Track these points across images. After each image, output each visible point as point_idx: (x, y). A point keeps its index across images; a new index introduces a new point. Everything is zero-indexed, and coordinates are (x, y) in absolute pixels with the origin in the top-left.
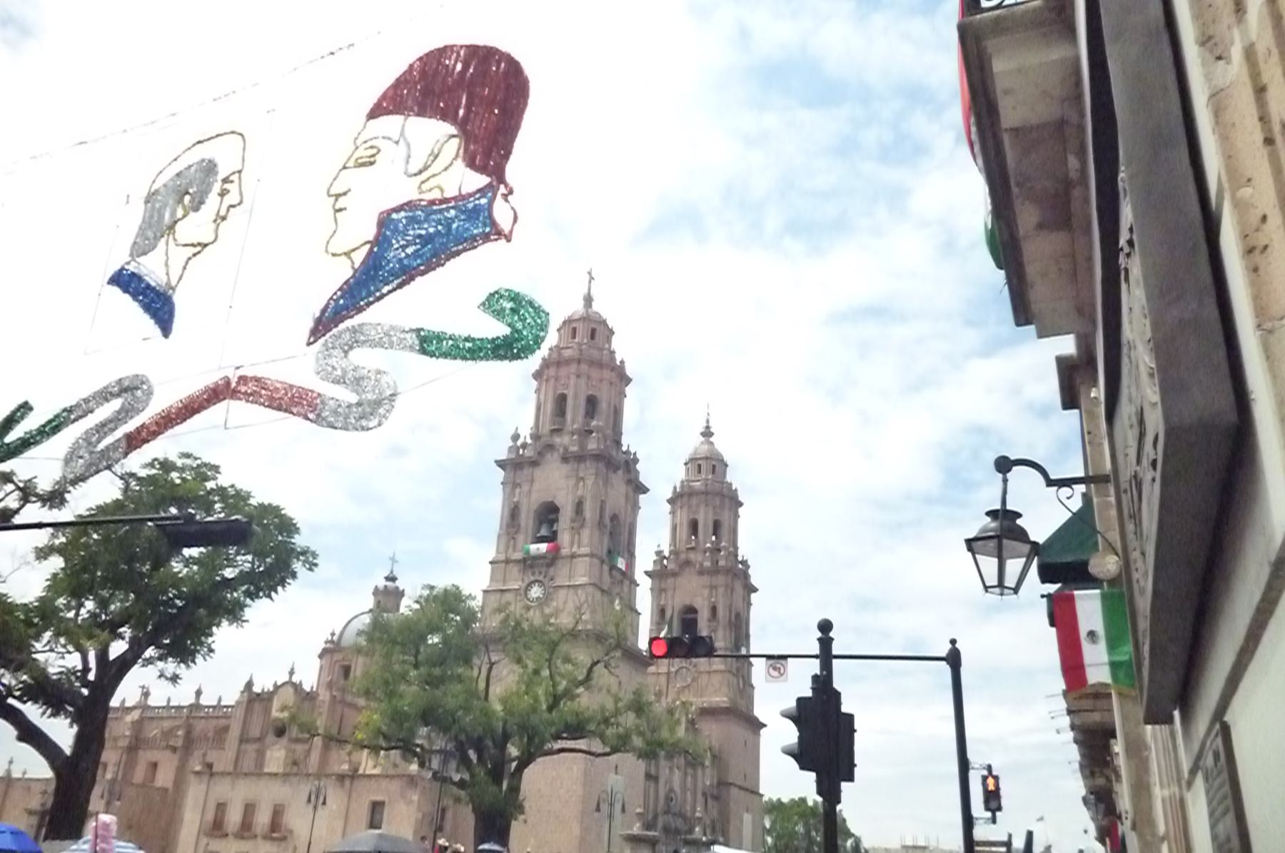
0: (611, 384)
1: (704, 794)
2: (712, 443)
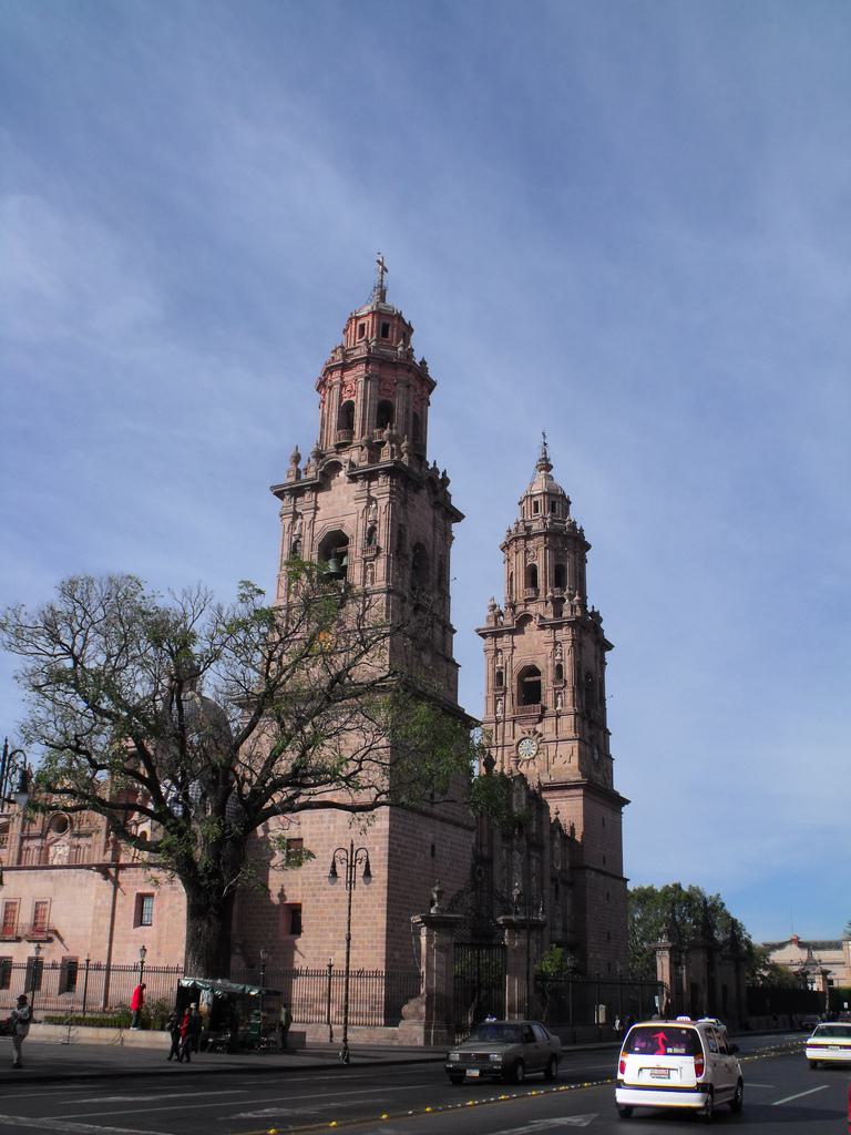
0: (408, 386)
1: (553, 880)
2: (551, 478)
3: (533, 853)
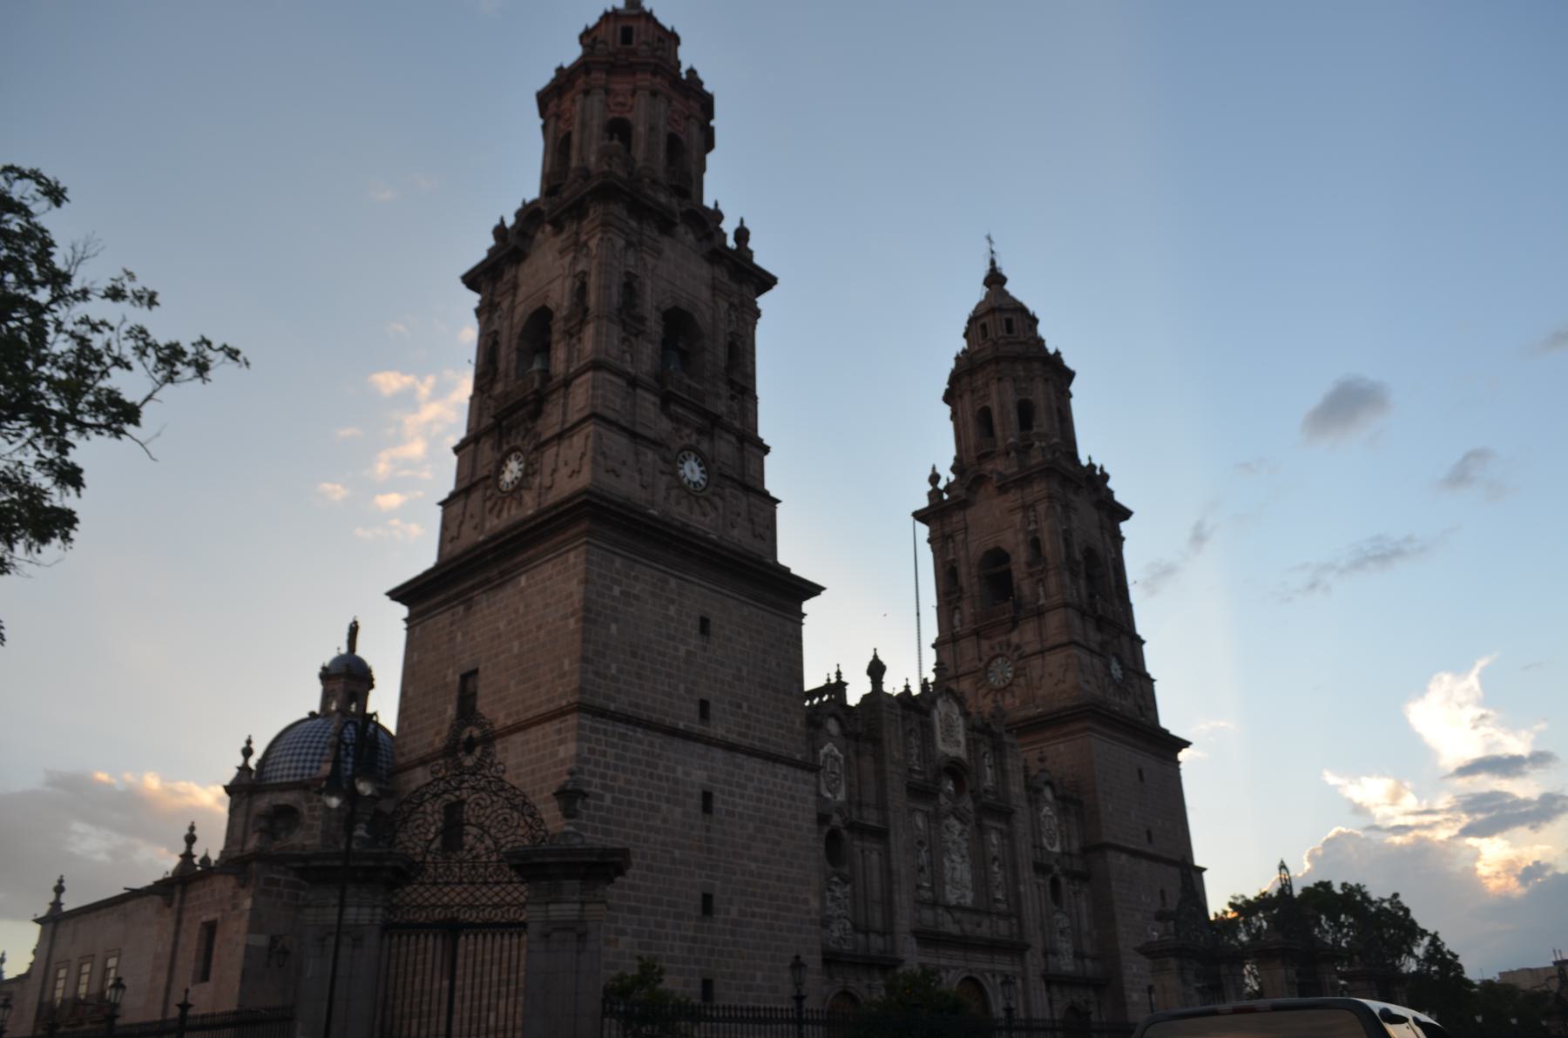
0: (654, 94)
1: (1040, 868)
3: (987, 822)
